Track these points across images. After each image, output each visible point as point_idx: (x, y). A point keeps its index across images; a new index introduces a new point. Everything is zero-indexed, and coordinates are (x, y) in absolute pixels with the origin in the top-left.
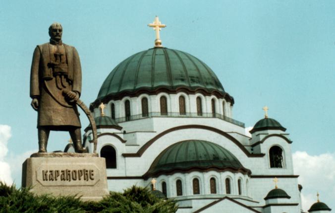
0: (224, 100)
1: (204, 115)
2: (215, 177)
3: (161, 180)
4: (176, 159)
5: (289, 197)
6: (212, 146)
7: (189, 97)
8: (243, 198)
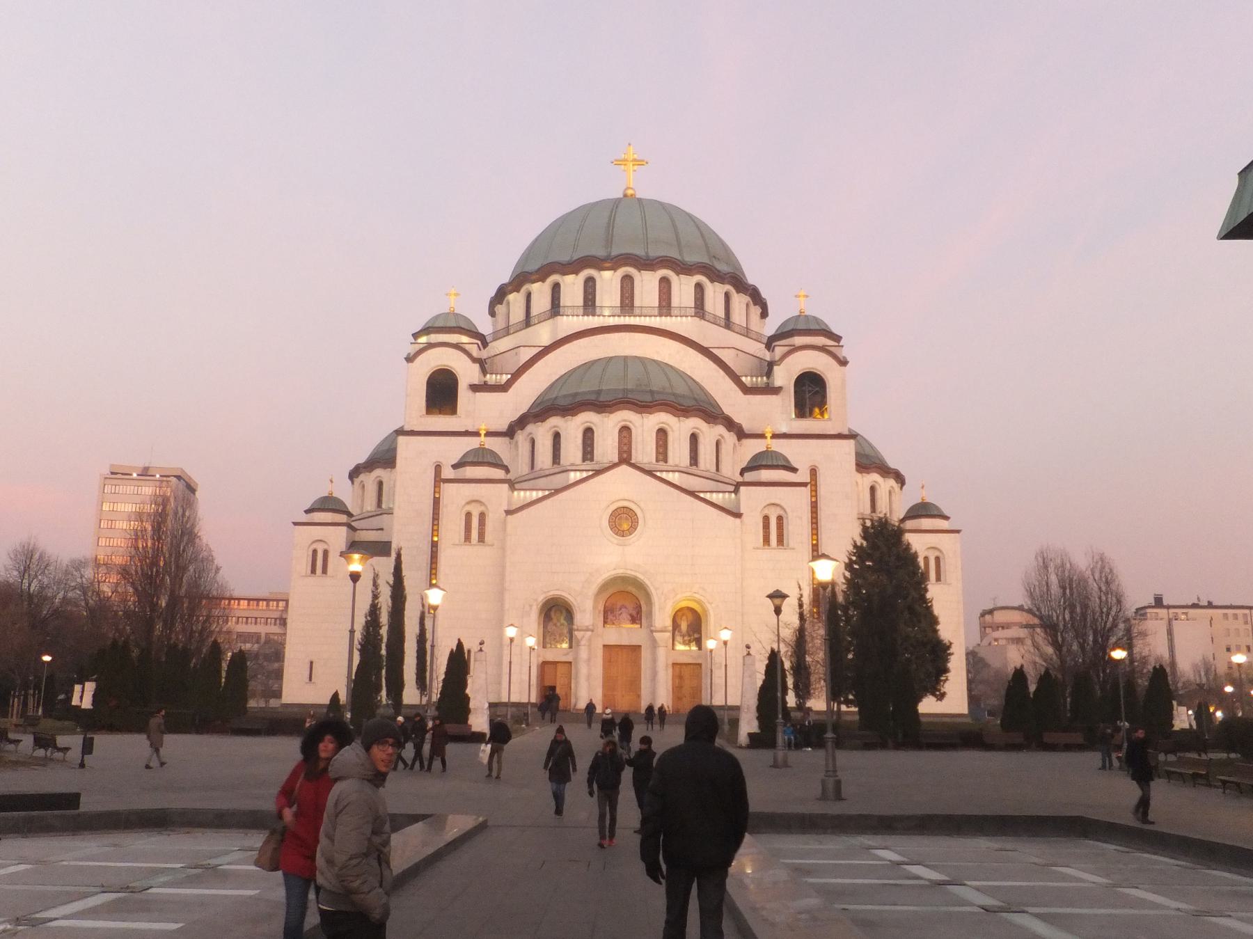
0: (728, 287)
1: (674, 312)
2: (628, 423)
3: (528, 436)
4: (560, 390)
5: (794, 470)
6: (663, 370)
7: (641, 276)
8: (704, 474)
